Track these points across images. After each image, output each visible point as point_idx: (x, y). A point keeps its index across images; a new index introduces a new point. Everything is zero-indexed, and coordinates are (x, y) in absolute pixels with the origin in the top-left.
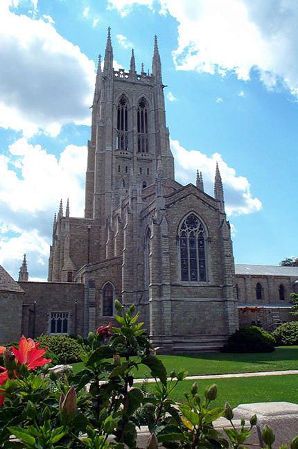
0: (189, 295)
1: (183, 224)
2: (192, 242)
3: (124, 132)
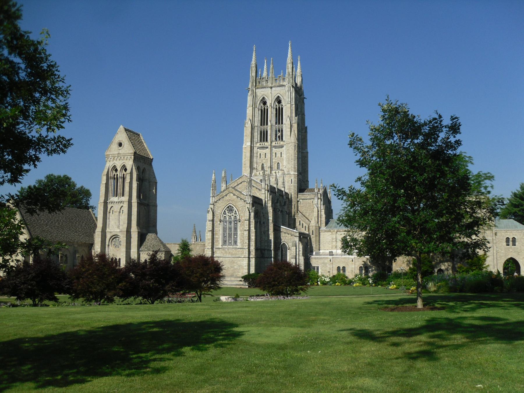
0: (225, 254)
1: (225, 211)
2: (230, 223)
3: (265, 126)
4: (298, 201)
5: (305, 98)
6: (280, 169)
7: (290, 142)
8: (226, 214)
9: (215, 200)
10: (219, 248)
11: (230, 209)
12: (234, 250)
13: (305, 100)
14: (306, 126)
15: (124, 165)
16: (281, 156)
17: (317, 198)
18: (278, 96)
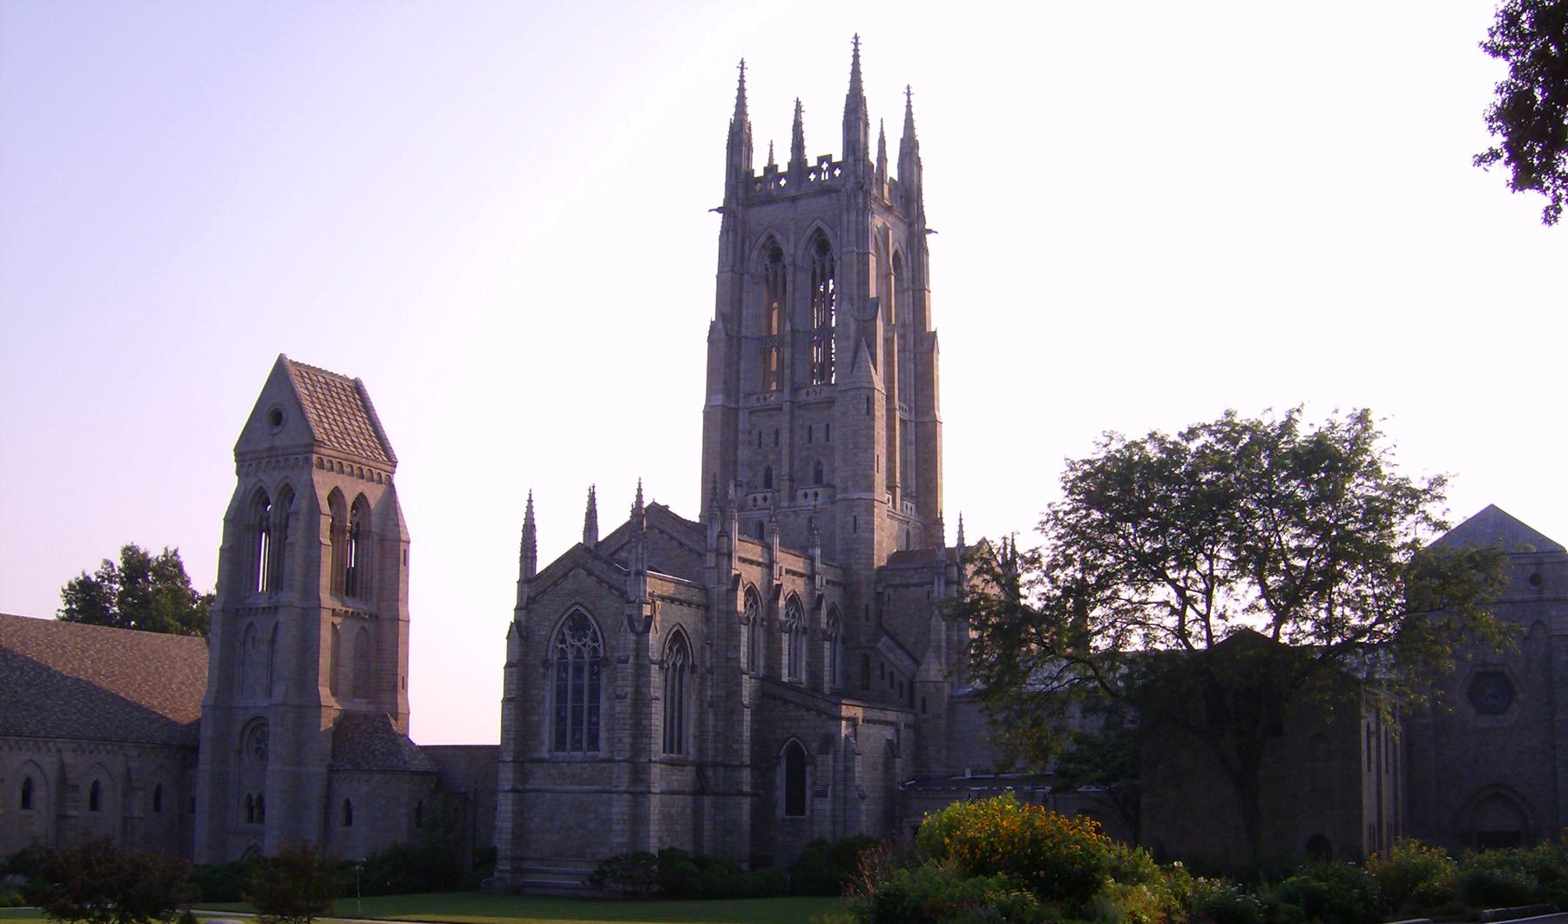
4: (878, 593)
5: (930, 231)
6: (824, 482)
7: (851, 386)
8: (563, 641)
9: (532, 595)
10: (541, 761)
11: (579, 624)
12: (587, 765)
13: (929, 237)
14: (933, 330)
15: (287, 485)
16: (827, 439)
17: (942, 582)
18: (819, 229)
